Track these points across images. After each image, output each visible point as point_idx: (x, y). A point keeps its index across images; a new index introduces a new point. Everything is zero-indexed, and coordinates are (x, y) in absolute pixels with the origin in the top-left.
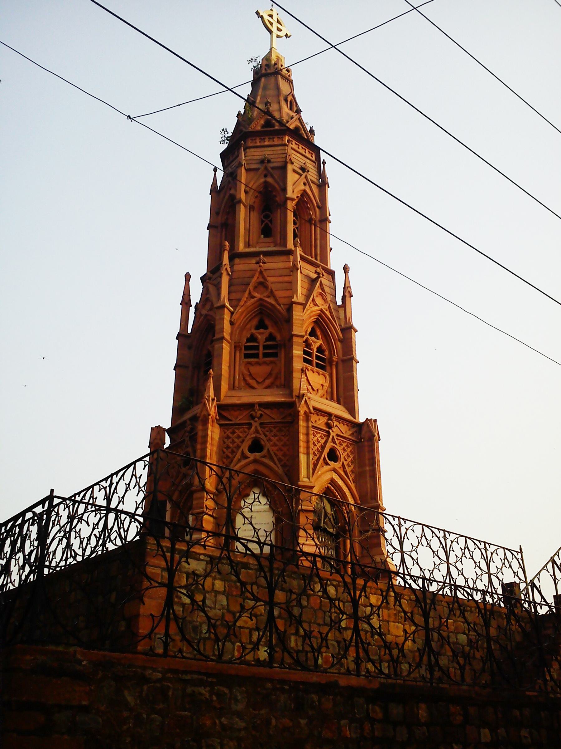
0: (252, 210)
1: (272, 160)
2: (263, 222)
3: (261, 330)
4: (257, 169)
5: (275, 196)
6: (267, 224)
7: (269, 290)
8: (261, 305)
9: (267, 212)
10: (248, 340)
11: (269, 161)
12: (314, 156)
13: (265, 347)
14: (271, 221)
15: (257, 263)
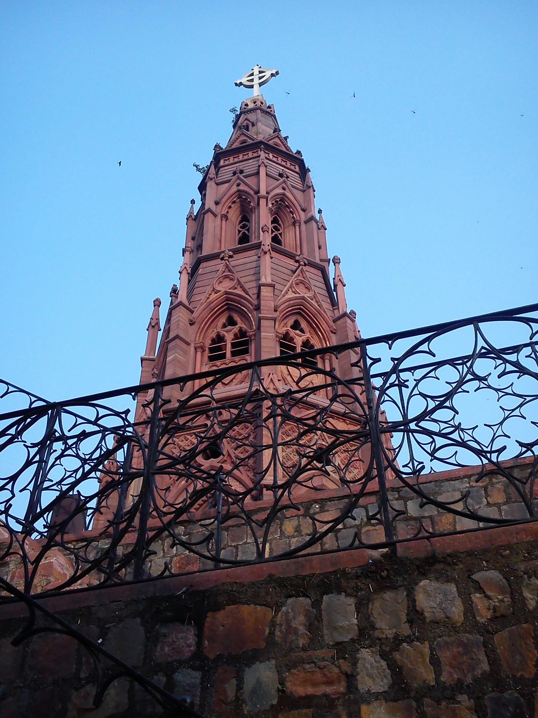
0: (223, 219)
1: (245, 171)
2: (239, 231)
3: (229, 327)
4: (228, 181)
5: (250, 202)
6: (244, 232)
7: (235, 281)
8: (228, 299)
9: (244, 223)
10: (213, 341)
11: (241, 172)
12: (297, 167)
13: (233, 345)
14: (248, 230)
15: (222, 259)
